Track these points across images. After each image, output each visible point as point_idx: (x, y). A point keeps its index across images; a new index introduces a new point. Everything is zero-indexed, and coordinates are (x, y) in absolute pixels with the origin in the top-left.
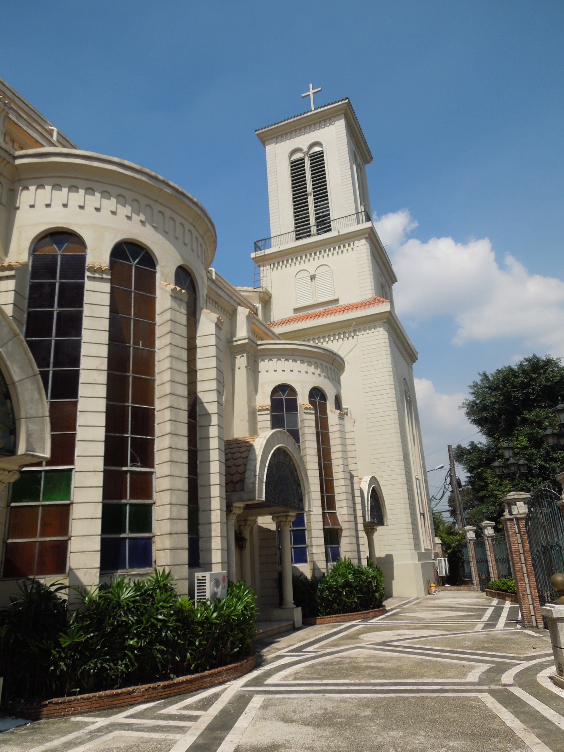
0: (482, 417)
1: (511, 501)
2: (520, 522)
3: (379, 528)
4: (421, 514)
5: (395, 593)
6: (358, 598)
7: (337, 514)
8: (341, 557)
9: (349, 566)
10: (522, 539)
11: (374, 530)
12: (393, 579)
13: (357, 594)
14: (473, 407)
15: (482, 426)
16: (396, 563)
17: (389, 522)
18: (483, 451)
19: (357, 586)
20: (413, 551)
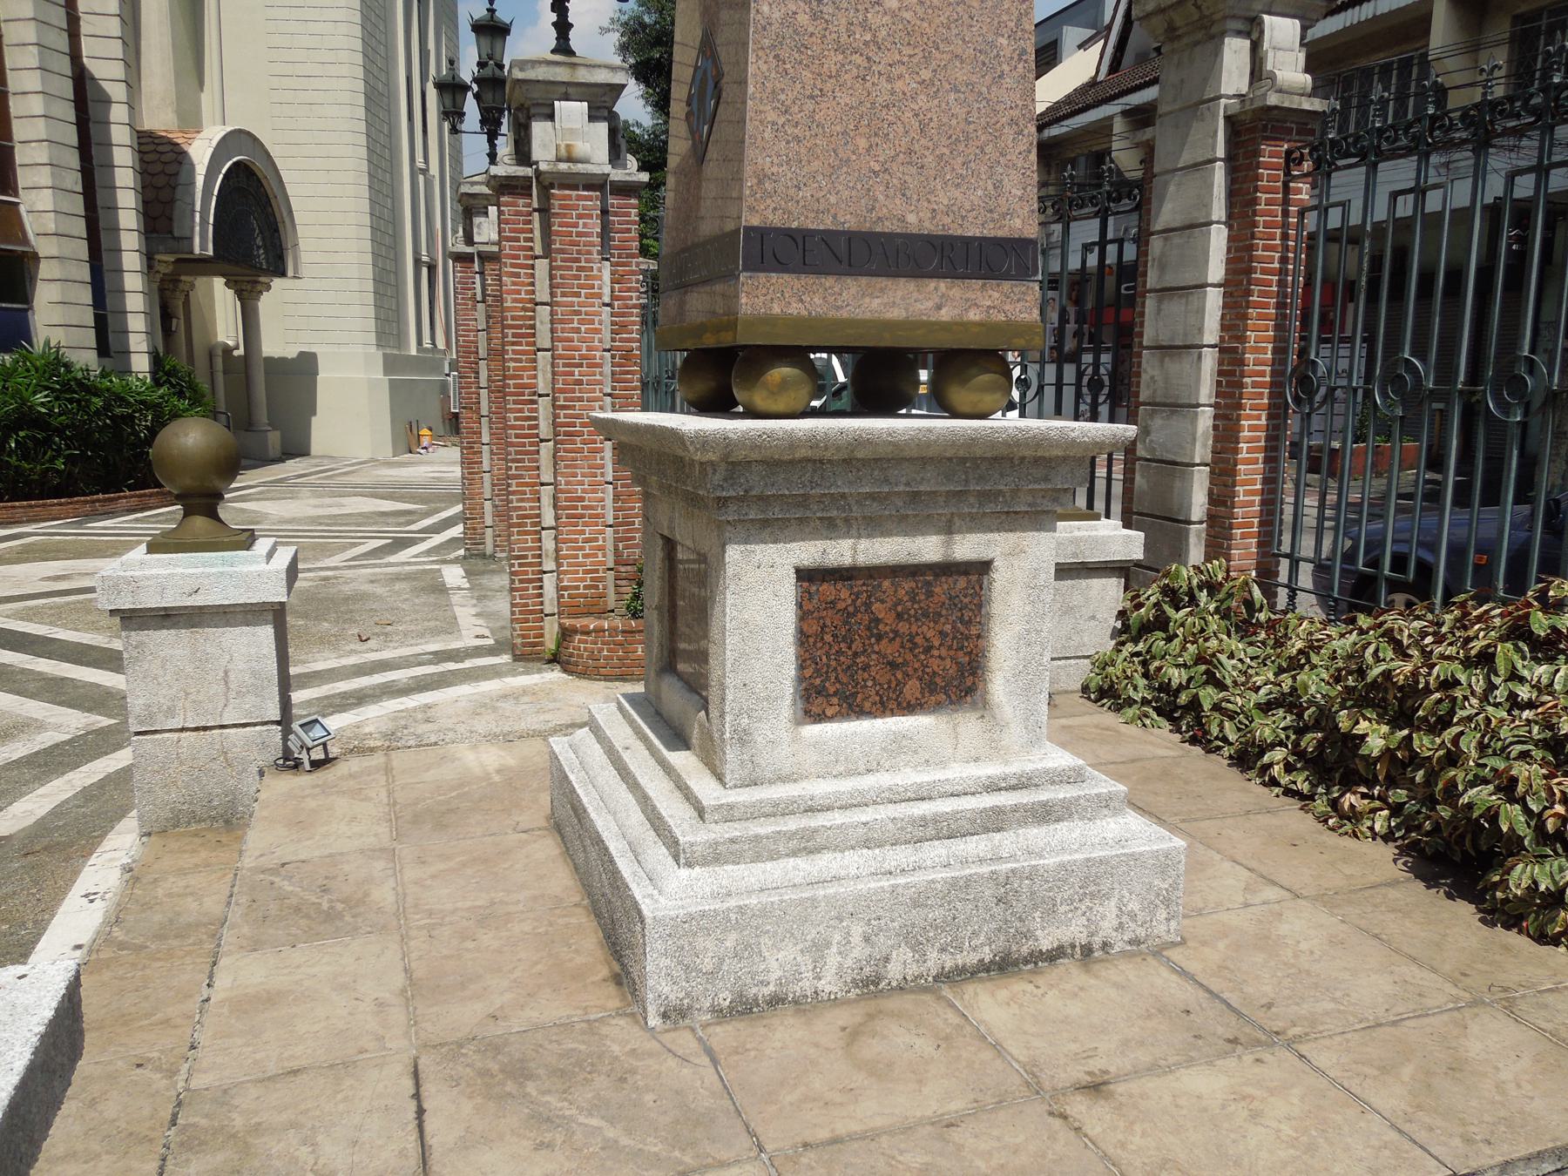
0: (649, 60)
1: (472, 201)
2: (488, 266)
3: (277, 283)
4: (417, 262)
5: (316, 446)
6: (70, 460)
7: (22, 209)
8: (35, 340)
9: (56, 364)
10: (488, 317)
11: (259, 287)
12: (315, 414)
13: (68, 448)
14: (634, 32)
15: (648, 85)
16: (323, 376)
17: (305, 270)
18: (641, 145)
19: (68, 427)
20: (373, 349)
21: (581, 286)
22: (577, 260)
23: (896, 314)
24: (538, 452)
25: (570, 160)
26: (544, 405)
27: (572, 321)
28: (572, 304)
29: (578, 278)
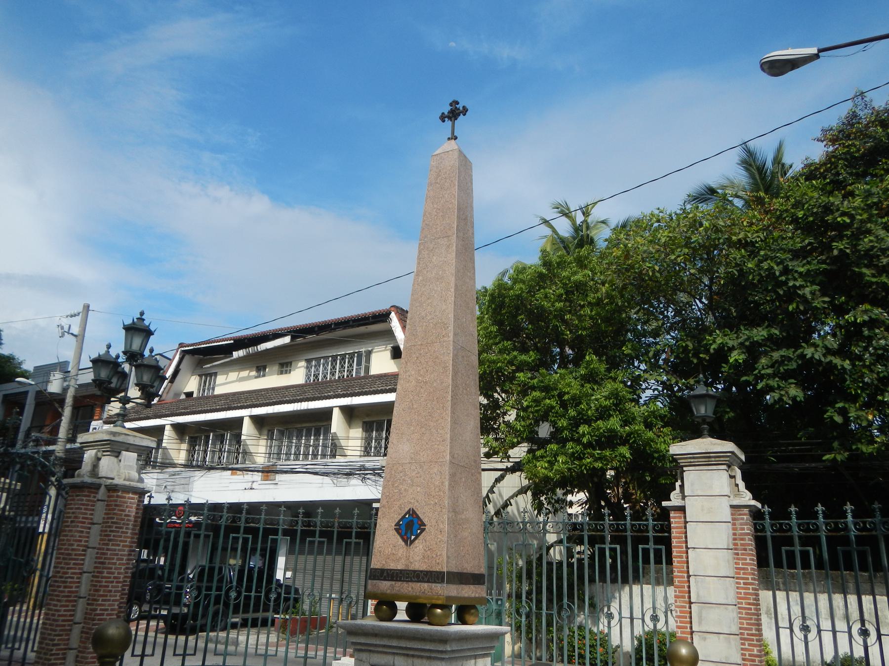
21: (121, 541)
22: (121, 528)
23: (466, 595)
24: (70, 630)
25: (129, 480)
26: (81, 605)
27: (113, 559)
28: (115, 550)
29: (121, 537)
